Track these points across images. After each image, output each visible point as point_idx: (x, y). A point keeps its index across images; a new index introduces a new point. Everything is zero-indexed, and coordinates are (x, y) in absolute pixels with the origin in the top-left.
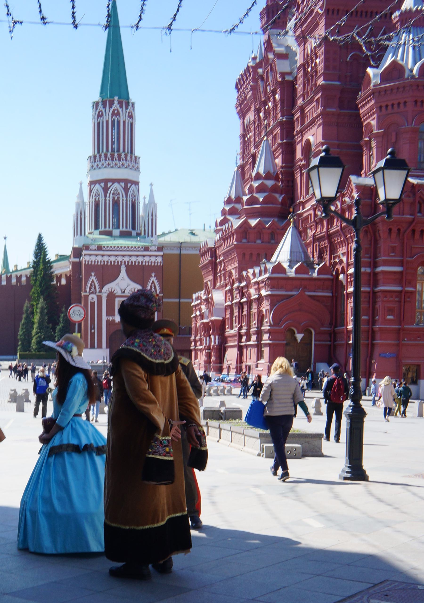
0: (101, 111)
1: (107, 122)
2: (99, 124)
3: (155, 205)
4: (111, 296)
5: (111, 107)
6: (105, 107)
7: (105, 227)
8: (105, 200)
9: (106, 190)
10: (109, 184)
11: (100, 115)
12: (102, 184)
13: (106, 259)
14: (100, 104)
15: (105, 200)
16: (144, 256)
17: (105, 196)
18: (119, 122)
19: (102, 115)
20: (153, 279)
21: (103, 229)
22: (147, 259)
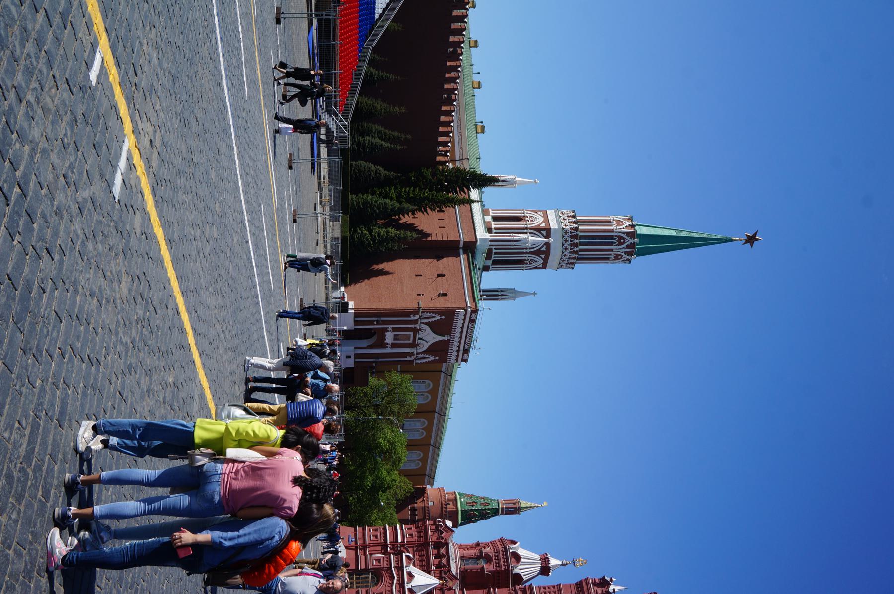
0: (624, 243)
1: (612, 250)
2: (611, 237)
3: (514, 298)
4: (416, 331)
5: (626, 253)
6: (628, 247)
7: (496, 253)
8: (526, 253)
9: (538, 253)
10: (543, 256)
11: (621, 240)
12: (544, 249)
13: (460, 325)
14: (632, 241)
15: (526, 253)
16: (458, 351)
17: (530, 253)
18: (608, 259)
19: (620, 244)
20: (432, 358)
21: (494, 251)
22: (455, 353)
